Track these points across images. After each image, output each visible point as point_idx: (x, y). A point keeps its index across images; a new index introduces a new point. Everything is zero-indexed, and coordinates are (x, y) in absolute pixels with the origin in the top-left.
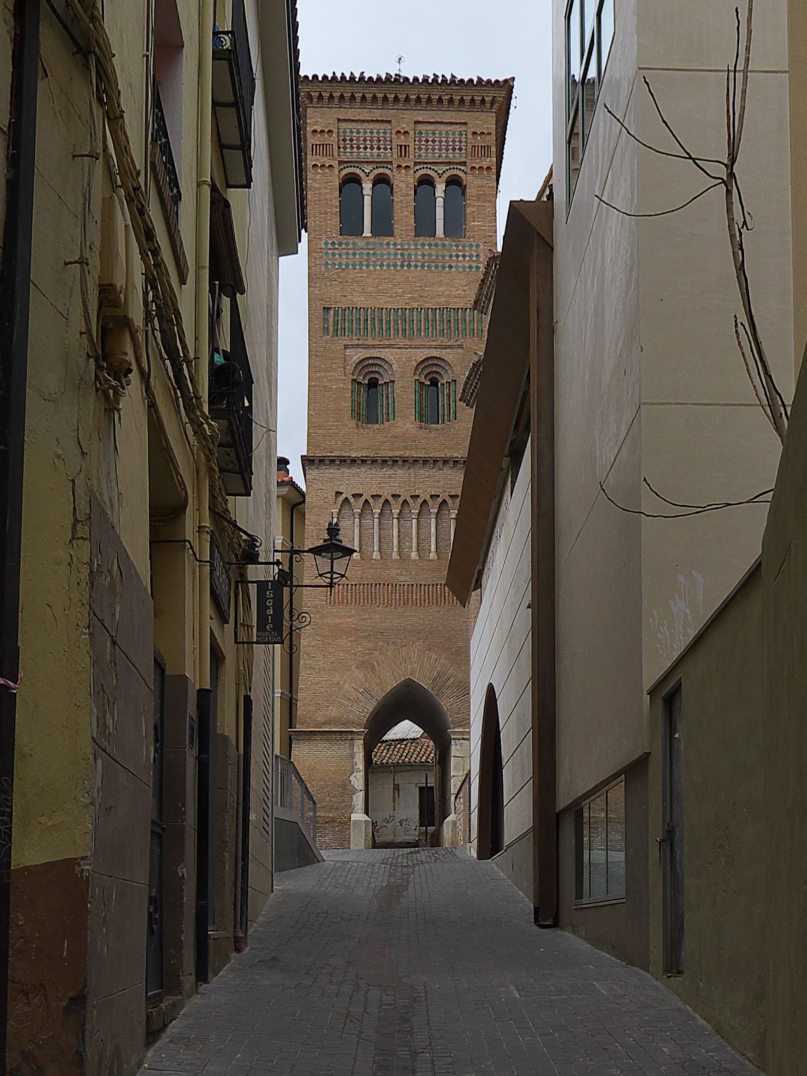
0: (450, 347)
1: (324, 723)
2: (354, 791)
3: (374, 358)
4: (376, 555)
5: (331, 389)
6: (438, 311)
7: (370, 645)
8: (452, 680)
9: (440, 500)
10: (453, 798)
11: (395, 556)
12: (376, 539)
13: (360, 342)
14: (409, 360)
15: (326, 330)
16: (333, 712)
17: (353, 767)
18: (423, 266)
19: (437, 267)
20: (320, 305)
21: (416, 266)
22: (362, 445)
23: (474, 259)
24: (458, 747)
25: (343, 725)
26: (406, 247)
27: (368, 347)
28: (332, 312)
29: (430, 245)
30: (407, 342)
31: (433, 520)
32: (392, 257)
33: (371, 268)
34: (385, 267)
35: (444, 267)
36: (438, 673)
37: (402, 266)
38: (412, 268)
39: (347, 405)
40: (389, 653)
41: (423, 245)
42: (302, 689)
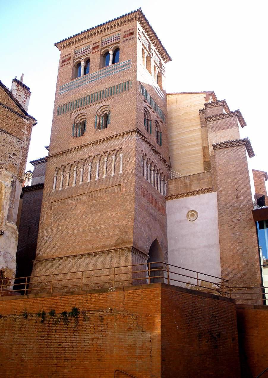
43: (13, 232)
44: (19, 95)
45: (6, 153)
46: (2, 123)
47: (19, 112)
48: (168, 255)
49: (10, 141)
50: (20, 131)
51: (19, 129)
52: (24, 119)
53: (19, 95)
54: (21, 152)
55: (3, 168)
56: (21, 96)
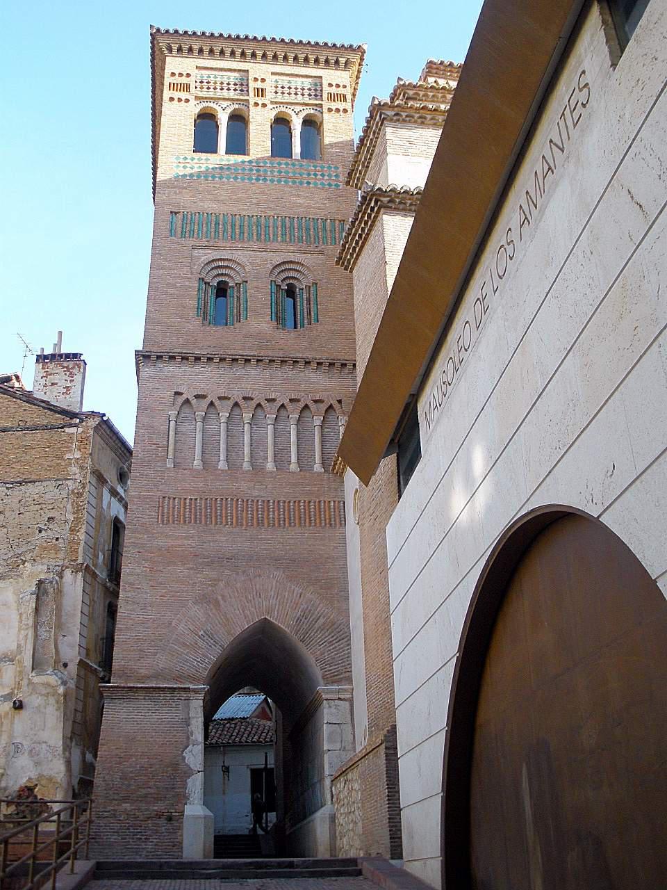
0: (310, 252)
1: (148, 677)
2: (189, 773)
3: (224, 260)
4: (222, 465)
5: (174, 286)
6: (296, 220)
7: (213, 574)
8: (322, 621)
9: (302, 405)
10: (327, 782)
11: (246, 466)
12: (223, 446)
13: (211, 244)
14: (265, 262)
15: (172, 232)
16: (162, 661)
17: (188, 738)
18: (279, 181)
19: (294, 182)
20: (167, 209)
21: (272, 181)
22: (208, 344)
23: (334, 178)
24: (333, 710)
25: (175, 679)
26: (262, 164)
27: (217, 248)
28: (180, 216)
29: (287, 164)
30: (263, 246)
31: (293, 427)
32: (247, 172)
33: (224, 180)
34: (239, 180)
35: (301, 183)
36: (304, 611)
37: (258, 180)
38: (268, 182)
39: (192, 302)
40: (239, 585)
41: (280, 164)
42: (121, 630)
43: (48, 693)
44: (53, 384)
45: (30, 526)
46: (14, 468)
47: (54, 422)
48: (349, 645)
49: (36, 497)
50: (59, 461)
51: (58, 458)
52: (67, 430)
53: (53, 384)
54: (69, 507)
55: (26, 561)
56: (56, 384)
